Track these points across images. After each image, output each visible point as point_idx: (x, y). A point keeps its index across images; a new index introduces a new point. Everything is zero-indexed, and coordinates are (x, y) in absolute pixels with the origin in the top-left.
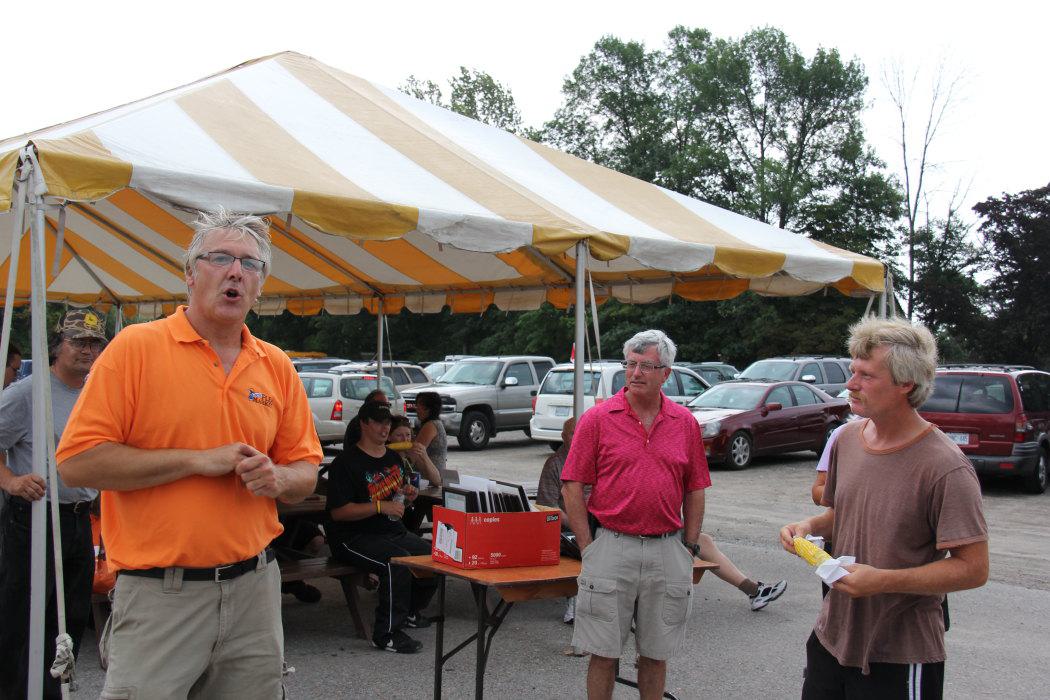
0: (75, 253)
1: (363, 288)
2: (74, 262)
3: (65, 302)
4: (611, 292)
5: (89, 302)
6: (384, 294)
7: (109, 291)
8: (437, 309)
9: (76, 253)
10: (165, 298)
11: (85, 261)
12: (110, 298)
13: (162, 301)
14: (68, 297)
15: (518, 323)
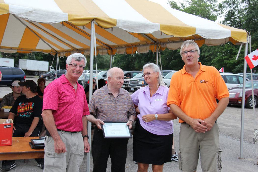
0: (40, 38)
1: (106, 47)
2: (40, 40)
3: (42, 52)
4: (166, 46)
5: (49, 52)
6: (112, 48)
7: (54, 50)
8: (123, 53)
9: (40, 38)
10: (66, 51)
11: (44, 40)
12: (54, 51)
13: (66, 52)
14: (42, 50)
15: (212, 62)
